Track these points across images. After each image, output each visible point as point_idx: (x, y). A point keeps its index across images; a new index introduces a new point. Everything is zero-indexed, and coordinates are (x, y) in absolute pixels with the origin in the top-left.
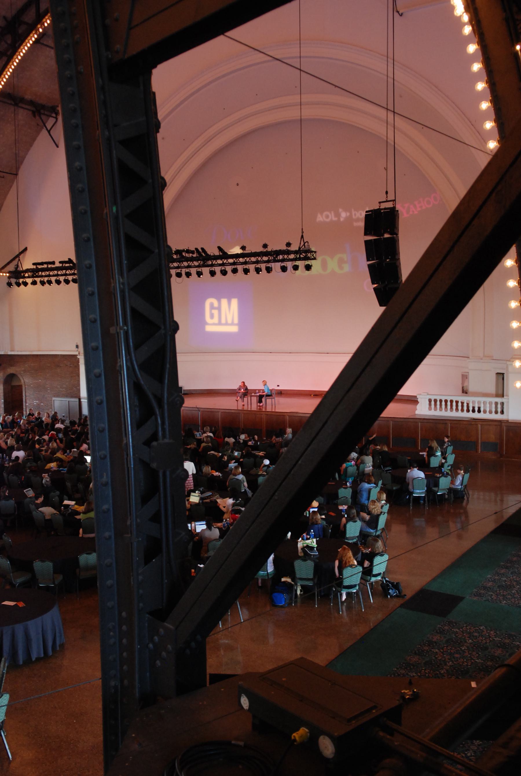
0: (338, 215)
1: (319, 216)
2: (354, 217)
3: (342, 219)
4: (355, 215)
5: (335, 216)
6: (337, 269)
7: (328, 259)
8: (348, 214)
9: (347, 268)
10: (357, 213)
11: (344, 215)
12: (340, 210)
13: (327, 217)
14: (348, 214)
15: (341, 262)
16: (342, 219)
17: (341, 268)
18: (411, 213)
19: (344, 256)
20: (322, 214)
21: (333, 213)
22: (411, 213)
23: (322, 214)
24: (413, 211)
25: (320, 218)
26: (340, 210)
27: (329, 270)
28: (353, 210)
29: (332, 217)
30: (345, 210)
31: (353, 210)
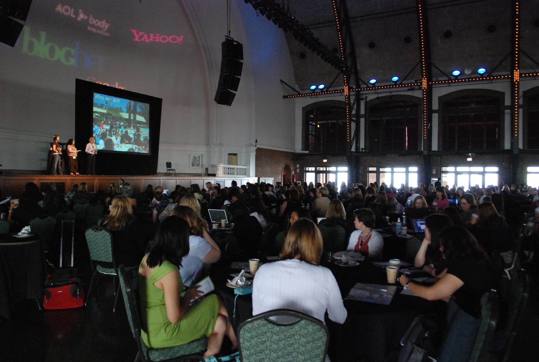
0: (77, 14)
1: (60, 6)
2: (90, 22)
3: (79, 19)
4: (92, 21)
5: (74, 13)
6: (63, 60)
7: (57, 48)
8: (86, 17)
9: (72, 62)
10: (93, 20)
11: (82, 16)
12: (80, 11)
13: (67, 11)
14: (86, 17)
15: (68, 55)
16: (79, 19)
17: (68, 61)
18: (143, 40)
19: (73, 51)
20: (62, 6)
21: (73, 10)
22: (143, 40)
23: (62, 6)
24: (145, 40)
25: (59, 9)
26: (80, 11)
27: (56, 58)
28: (91, 16)
29: (71, 13)
30: (85, 13)
31: (91, 16)
